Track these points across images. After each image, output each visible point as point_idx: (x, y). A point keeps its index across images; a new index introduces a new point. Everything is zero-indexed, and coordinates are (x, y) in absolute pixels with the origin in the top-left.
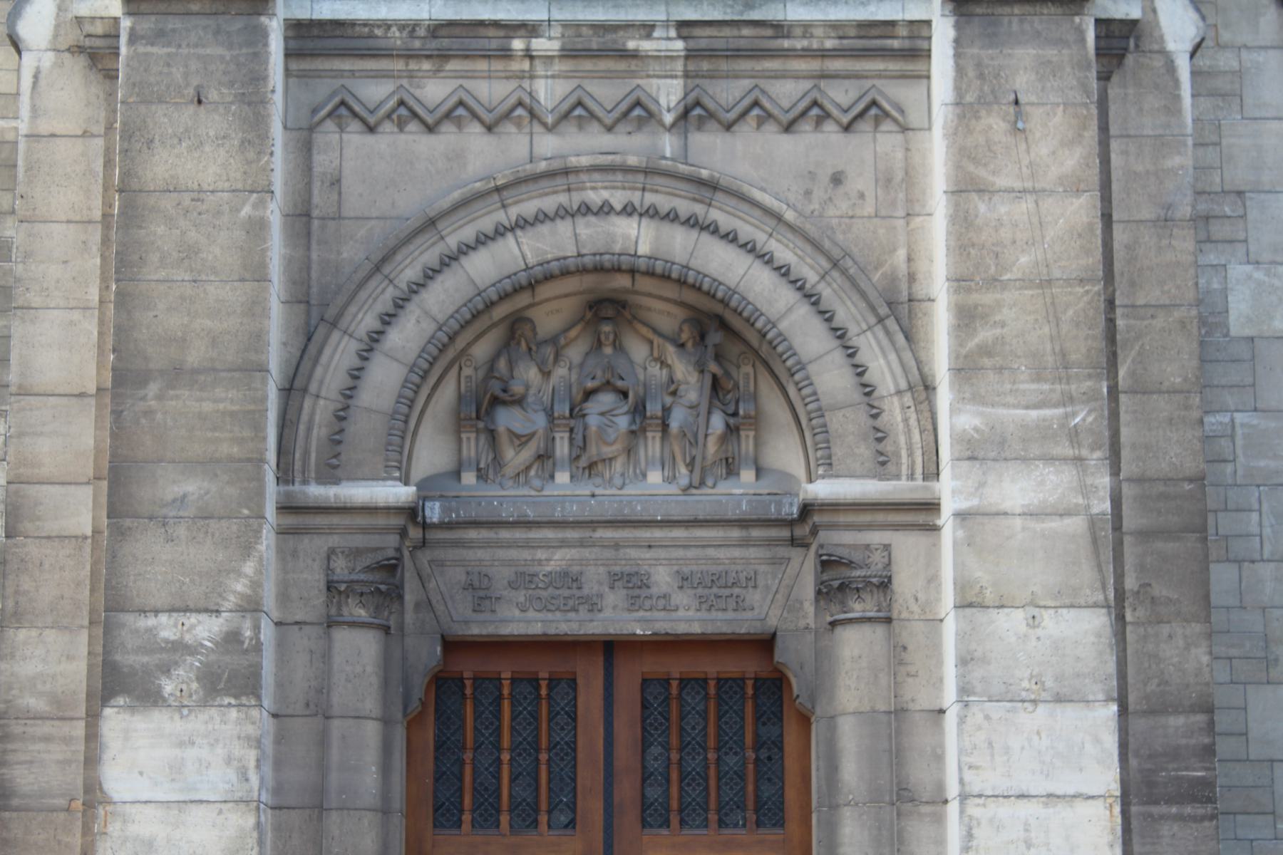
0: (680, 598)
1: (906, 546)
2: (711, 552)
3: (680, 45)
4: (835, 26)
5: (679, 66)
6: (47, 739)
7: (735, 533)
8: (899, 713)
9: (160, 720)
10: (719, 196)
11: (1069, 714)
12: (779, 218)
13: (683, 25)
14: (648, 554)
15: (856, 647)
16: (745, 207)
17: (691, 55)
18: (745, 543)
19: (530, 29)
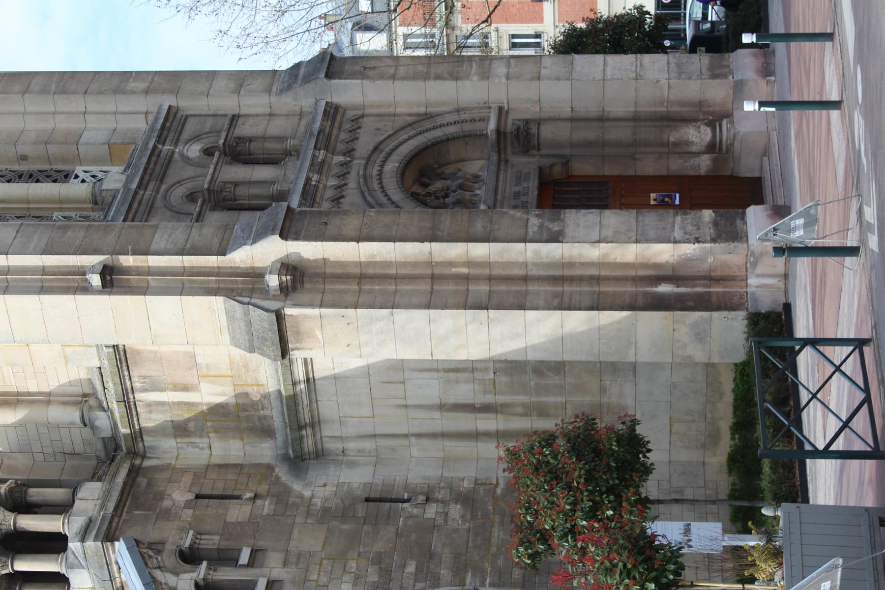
0: (525, 185)
1: (512, 116)
2: (508, 179)
3: (322, 151)
4: (323, 120)
5: (329, 155)
6: (570, 299)
7: (502, 172)
8: (572, 120)
9: (567, 230)
10: (380, 147)
11: (575, 62)
12: (390, 136)
13: (315, 147)
14: (508, 191)
15: (547, 132)
16: (385, 142)
17: (326, 148)
18: (506, 171)
19: (308, 180)
